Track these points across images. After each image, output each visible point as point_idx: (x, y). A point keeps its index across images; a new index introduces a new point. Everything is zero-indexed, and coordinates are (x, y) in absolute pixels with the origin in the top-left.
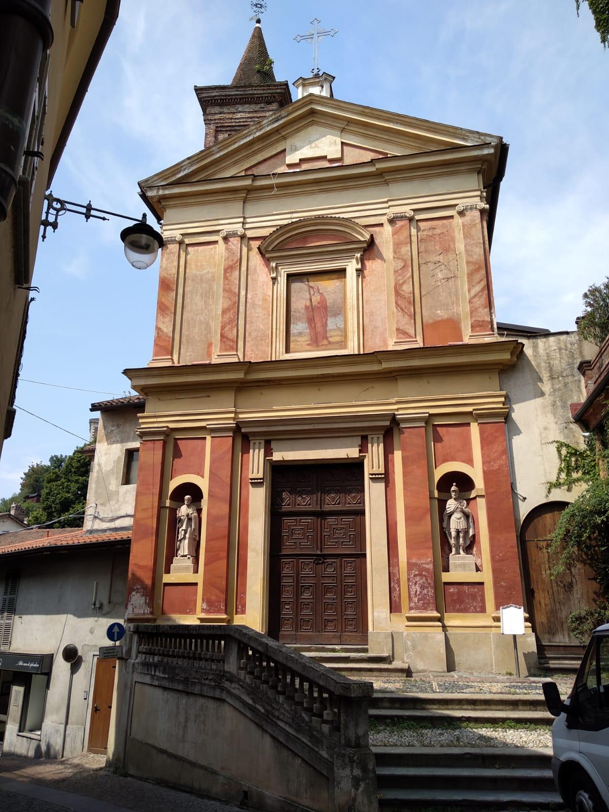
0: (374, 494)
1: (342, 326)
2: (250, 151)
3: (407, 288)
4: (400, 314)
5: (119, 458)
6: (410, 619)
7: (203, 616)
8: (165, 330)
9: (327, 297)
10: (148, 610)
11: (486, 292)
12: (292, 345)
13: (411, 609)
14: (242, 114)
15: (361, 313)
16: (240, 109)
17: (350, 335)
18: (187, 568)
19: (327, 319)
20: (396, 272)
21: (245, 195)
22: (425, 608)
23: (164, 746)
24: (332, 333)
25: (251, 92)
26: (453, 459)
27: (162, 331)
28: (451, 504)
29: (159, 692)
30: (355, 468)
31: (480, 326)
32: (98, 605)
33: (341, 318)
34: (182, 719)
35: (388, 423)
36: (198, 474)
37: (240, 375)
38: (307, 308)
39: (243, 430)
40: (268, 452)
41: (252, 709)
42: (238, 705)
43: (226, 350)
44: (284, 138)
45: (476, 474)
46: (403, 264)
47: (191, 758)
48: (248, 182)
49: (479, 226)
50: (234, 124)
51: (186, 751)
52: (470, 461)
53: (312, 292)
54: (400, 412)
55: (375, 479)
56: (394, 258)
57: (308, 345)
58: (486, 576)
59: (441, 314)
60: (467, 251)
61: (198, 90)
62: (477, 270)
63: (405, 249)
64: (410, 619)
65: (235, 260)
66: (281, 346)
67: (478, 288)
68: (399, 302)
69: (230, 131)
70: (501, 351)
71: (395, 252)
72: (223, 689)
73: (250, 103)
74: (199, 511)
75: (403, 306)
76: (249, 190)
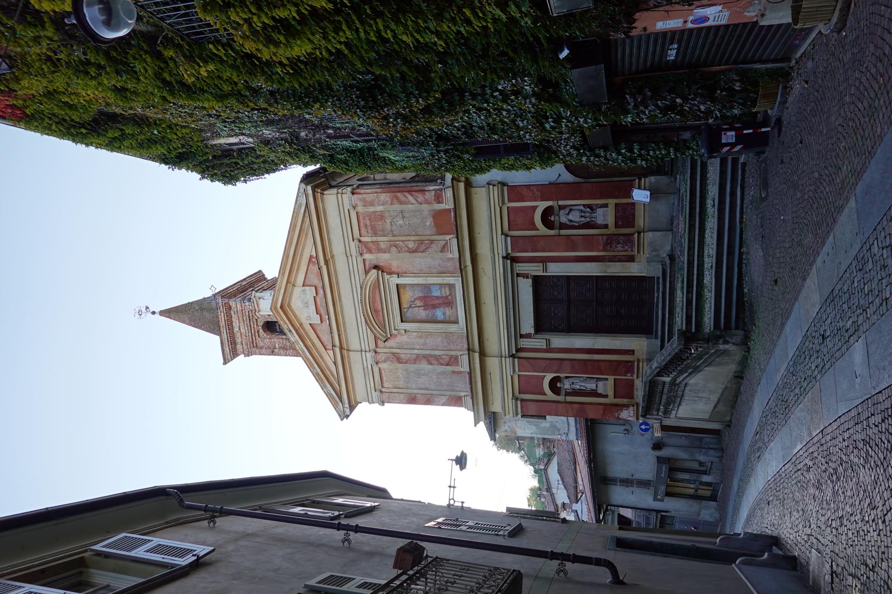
0: (556, 269)
1: (438, 286)
2: (313, 347)
3: (411, 245)
4: (430, 250)
5: (527, 422)
6: (639, 252)
7: (635, 376)
8: (444, 401)
9: (417, 296)
10: (631, 408)
11: (413, 193)
12: (452, 319)
13: (632, 250)
14: (241, 329)
15: (429, 274)
16: (238, 329)
17: (445, 282)
18: (605, 384)
19: (434, 296)
20: (399, 252)
21: (345, 351)
22: (632, 242)
23: (713, 405)
24: (443, 293)
25: (223, 322)
26: (533, 218)
27: (445, 402)
28: (564, 219)
29: (681, 407)
30: (538, 282)
31: (438, 198)
32: (626, 432)
33: (432, 287)
34: (697, 399)
35: (509, 261)
36: (543, 379)
37: (477, 355)
38: (425, 309)
39: (514, 352)
40: (528, 336)
41: (690, 374)
42: (688, 378)
43: (458, 362)
44: (301, 325)
45: (542, 205)
46: (394, 247)
47: (718, 395)
48: (337, 350)
49: (364, 196)
50: (250, 334)
51: (714, 398)
52: (534, 208)
53: (414, 306)
54: (500, 252)
55: (545, 269)
56: (389, 253)
57: (452, 308)
58: (612, 202)
59: (429, 222)
60: (383, 204)
61: (225, 363)
62: (397, 198)
63: (383, 246)
64: (639, 252)
65: (393, 356)
66: (453, 328)
67: (411, 198)
68: (422, 250)
69: (255, 337)
70: (458, 189)
71: (385, 252)
72: (680, 383)
73: (232, 322)
74: (567, 377)
75: (425, 248)
76: (341, 348)
